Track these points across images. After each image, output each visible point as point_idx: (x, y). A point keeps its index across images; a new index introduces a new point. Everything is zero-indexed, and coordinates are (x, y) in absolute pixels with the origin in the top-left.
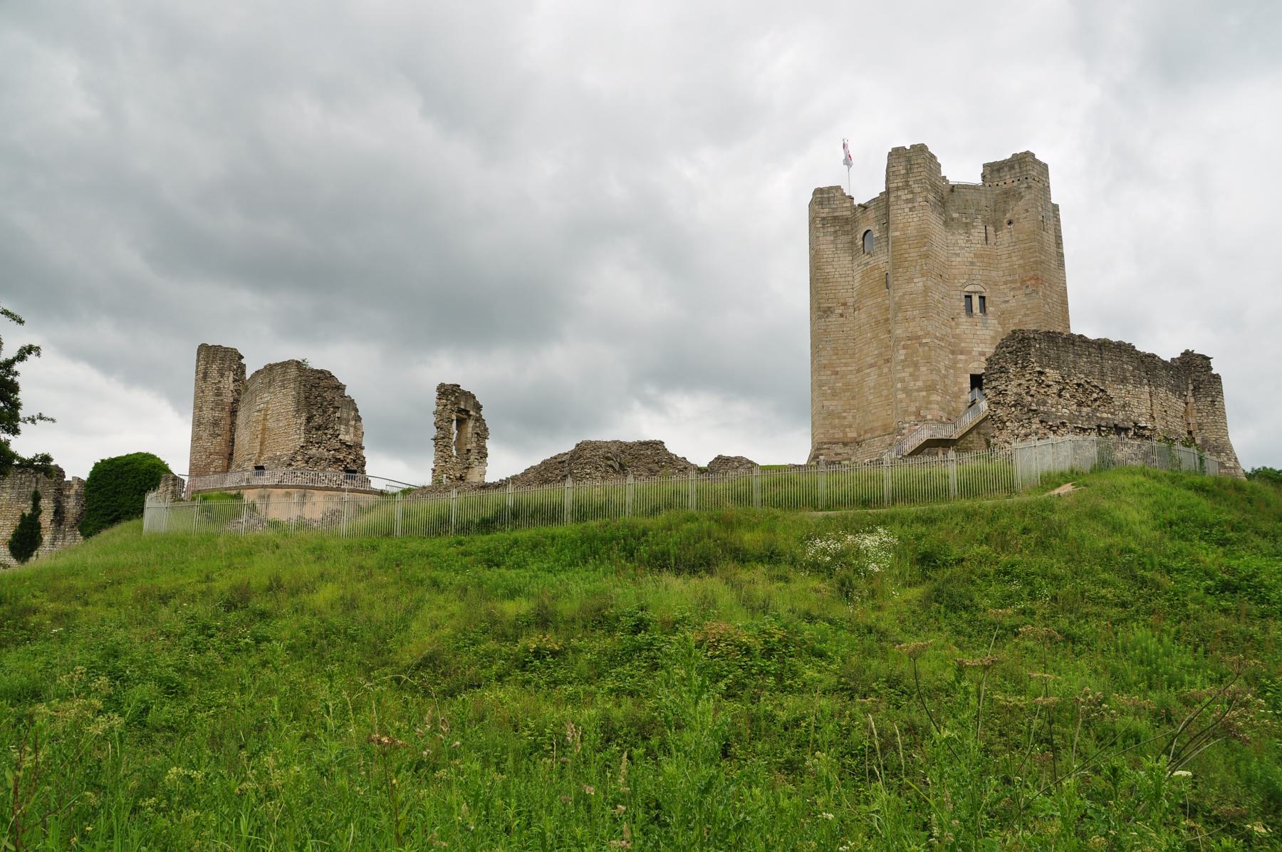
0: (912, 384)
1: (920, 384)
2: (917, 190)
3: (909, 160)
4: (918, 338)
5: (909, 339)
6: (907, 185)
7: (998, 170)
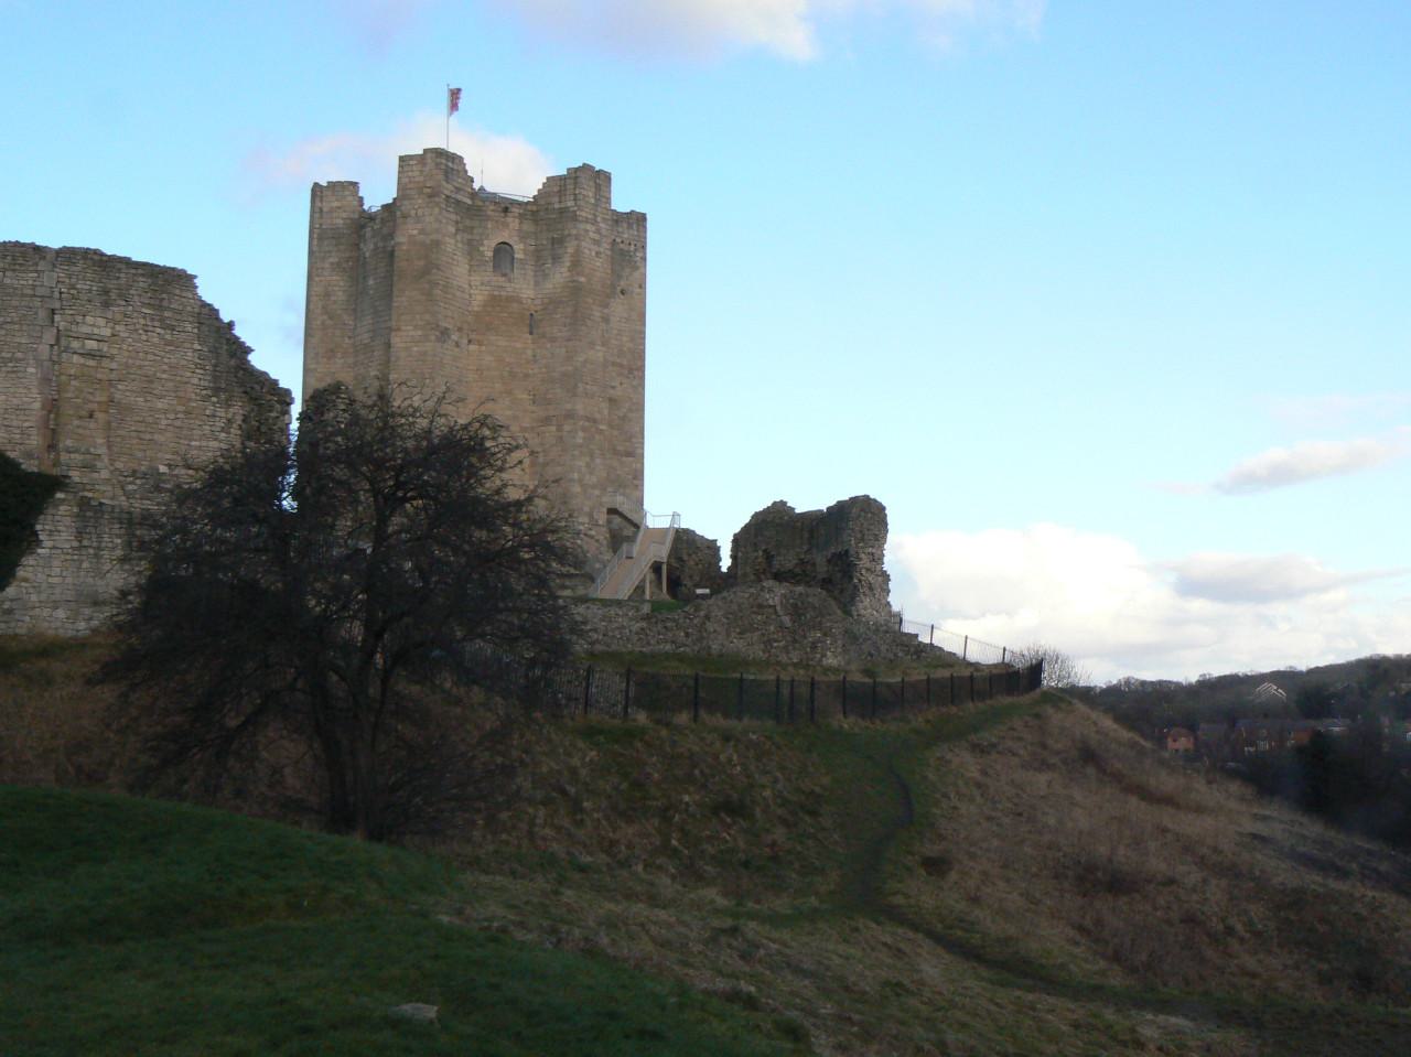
0: (587, 477)
1: (594, 479)
2: (604, 232)
3: (598, 187)
4: (595, 421)
5: (588, 419)
6: (594, 222)
7: (617, 222)
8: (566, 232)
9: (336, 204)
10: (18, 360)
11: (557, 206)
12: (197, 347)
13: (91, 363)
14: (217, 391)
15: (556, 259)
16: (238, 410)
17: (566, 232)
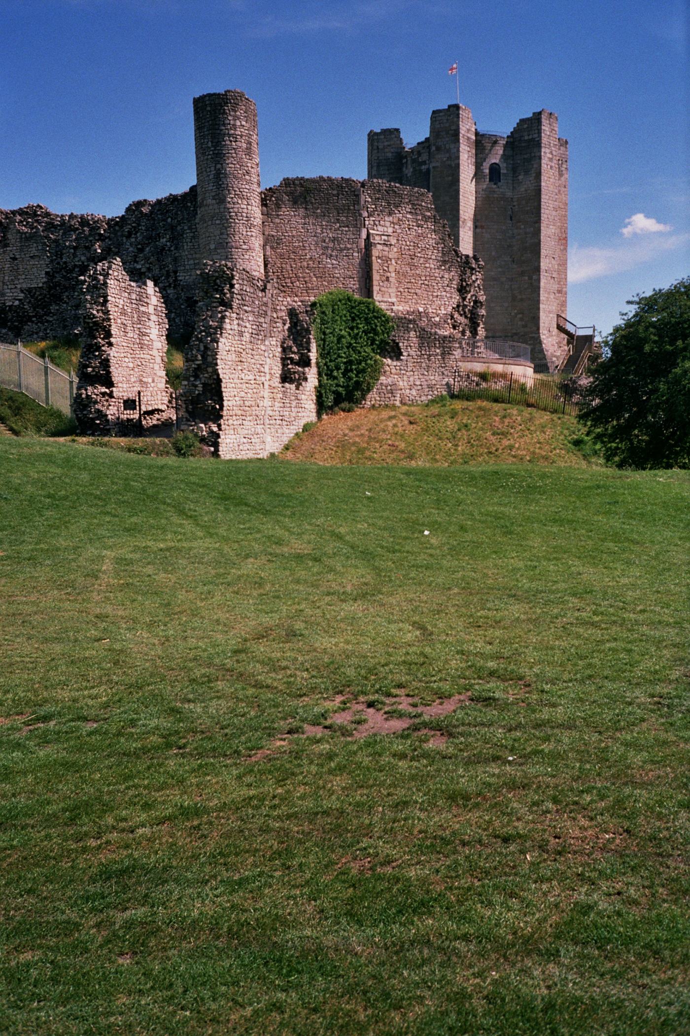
2: (554, 153)
8: (533, 155)
9: (386, 144)
10: (348, 249)
11: (526, 138)
12: (434, 236)
13: (386, 249)
14: (444, 262)
15: (527, 172)
16: (454, 274)
17: (533, 155)
